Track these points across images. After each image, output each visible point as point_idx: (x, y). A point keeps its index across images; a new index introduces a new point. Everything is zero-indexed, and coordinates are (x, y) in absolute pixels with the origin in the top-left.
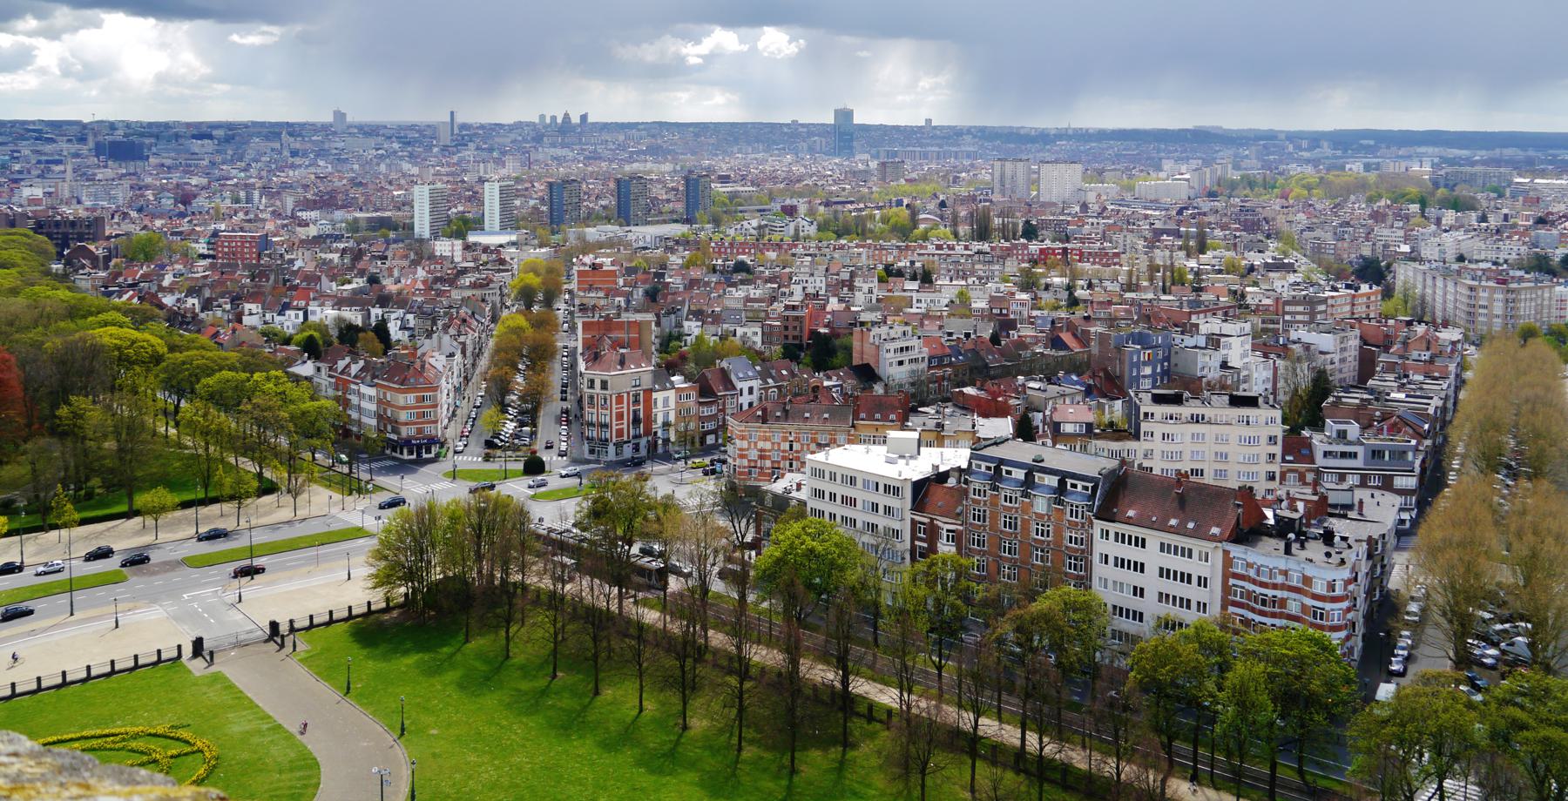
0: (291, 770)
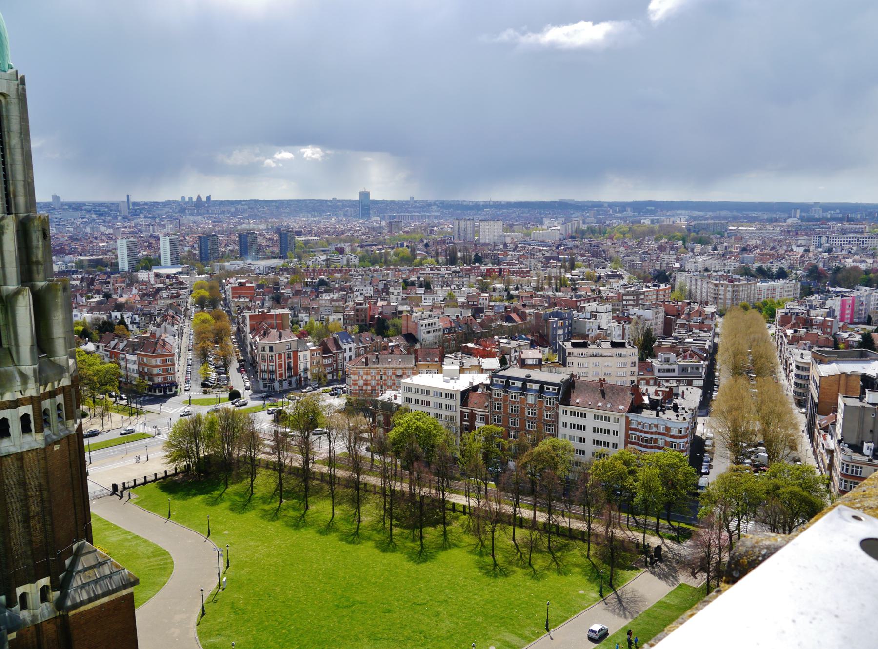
0: (154, 556)
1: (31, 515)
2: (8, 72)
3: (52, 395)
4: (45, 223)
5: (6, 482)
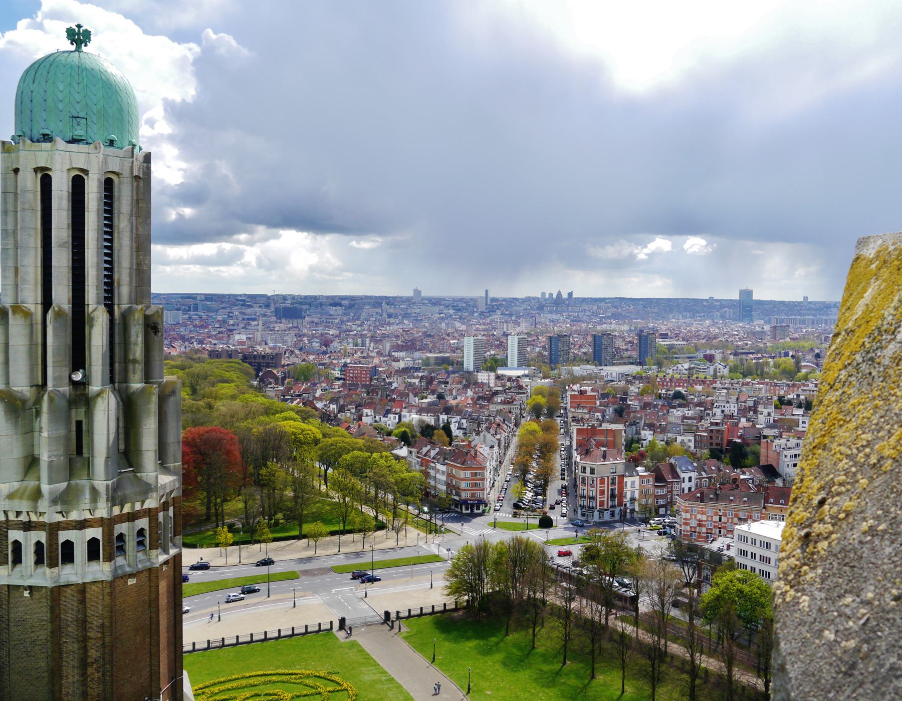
1: (89, 660)
3: (132, 517)
5: (63, 616)
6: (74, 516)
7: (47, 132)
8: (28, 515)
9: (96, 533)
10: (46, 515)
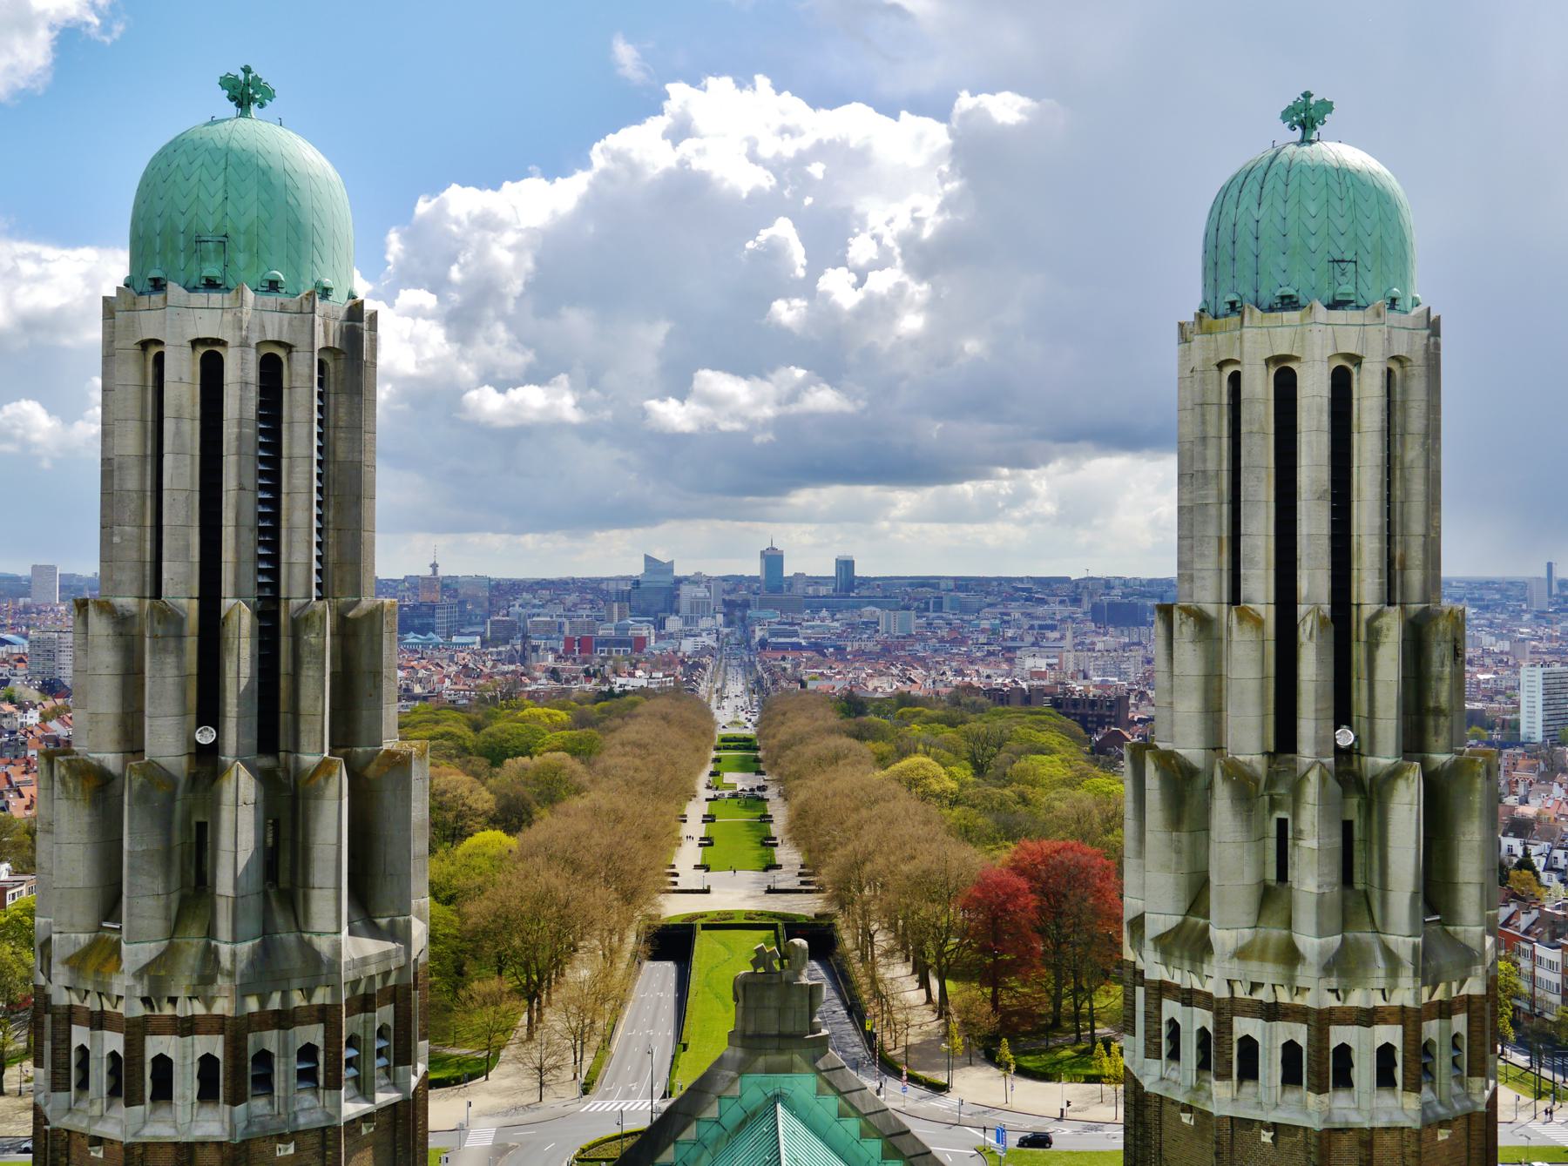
2: (1413, 313)
3: (1444, 1010)
4: (1459, 621)
6: (1357, 999)
7: (1292, 292)
8: (1274, 991)
9: (1389, 1034)
10: (1308, 994)
